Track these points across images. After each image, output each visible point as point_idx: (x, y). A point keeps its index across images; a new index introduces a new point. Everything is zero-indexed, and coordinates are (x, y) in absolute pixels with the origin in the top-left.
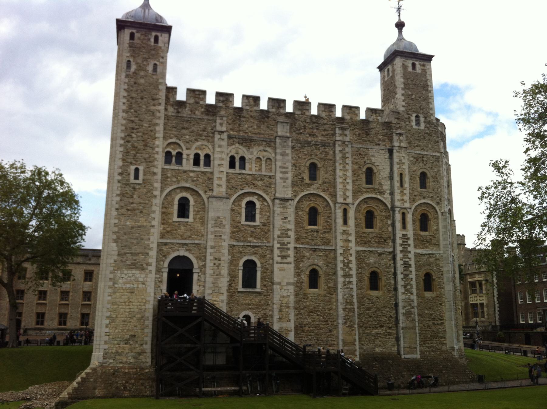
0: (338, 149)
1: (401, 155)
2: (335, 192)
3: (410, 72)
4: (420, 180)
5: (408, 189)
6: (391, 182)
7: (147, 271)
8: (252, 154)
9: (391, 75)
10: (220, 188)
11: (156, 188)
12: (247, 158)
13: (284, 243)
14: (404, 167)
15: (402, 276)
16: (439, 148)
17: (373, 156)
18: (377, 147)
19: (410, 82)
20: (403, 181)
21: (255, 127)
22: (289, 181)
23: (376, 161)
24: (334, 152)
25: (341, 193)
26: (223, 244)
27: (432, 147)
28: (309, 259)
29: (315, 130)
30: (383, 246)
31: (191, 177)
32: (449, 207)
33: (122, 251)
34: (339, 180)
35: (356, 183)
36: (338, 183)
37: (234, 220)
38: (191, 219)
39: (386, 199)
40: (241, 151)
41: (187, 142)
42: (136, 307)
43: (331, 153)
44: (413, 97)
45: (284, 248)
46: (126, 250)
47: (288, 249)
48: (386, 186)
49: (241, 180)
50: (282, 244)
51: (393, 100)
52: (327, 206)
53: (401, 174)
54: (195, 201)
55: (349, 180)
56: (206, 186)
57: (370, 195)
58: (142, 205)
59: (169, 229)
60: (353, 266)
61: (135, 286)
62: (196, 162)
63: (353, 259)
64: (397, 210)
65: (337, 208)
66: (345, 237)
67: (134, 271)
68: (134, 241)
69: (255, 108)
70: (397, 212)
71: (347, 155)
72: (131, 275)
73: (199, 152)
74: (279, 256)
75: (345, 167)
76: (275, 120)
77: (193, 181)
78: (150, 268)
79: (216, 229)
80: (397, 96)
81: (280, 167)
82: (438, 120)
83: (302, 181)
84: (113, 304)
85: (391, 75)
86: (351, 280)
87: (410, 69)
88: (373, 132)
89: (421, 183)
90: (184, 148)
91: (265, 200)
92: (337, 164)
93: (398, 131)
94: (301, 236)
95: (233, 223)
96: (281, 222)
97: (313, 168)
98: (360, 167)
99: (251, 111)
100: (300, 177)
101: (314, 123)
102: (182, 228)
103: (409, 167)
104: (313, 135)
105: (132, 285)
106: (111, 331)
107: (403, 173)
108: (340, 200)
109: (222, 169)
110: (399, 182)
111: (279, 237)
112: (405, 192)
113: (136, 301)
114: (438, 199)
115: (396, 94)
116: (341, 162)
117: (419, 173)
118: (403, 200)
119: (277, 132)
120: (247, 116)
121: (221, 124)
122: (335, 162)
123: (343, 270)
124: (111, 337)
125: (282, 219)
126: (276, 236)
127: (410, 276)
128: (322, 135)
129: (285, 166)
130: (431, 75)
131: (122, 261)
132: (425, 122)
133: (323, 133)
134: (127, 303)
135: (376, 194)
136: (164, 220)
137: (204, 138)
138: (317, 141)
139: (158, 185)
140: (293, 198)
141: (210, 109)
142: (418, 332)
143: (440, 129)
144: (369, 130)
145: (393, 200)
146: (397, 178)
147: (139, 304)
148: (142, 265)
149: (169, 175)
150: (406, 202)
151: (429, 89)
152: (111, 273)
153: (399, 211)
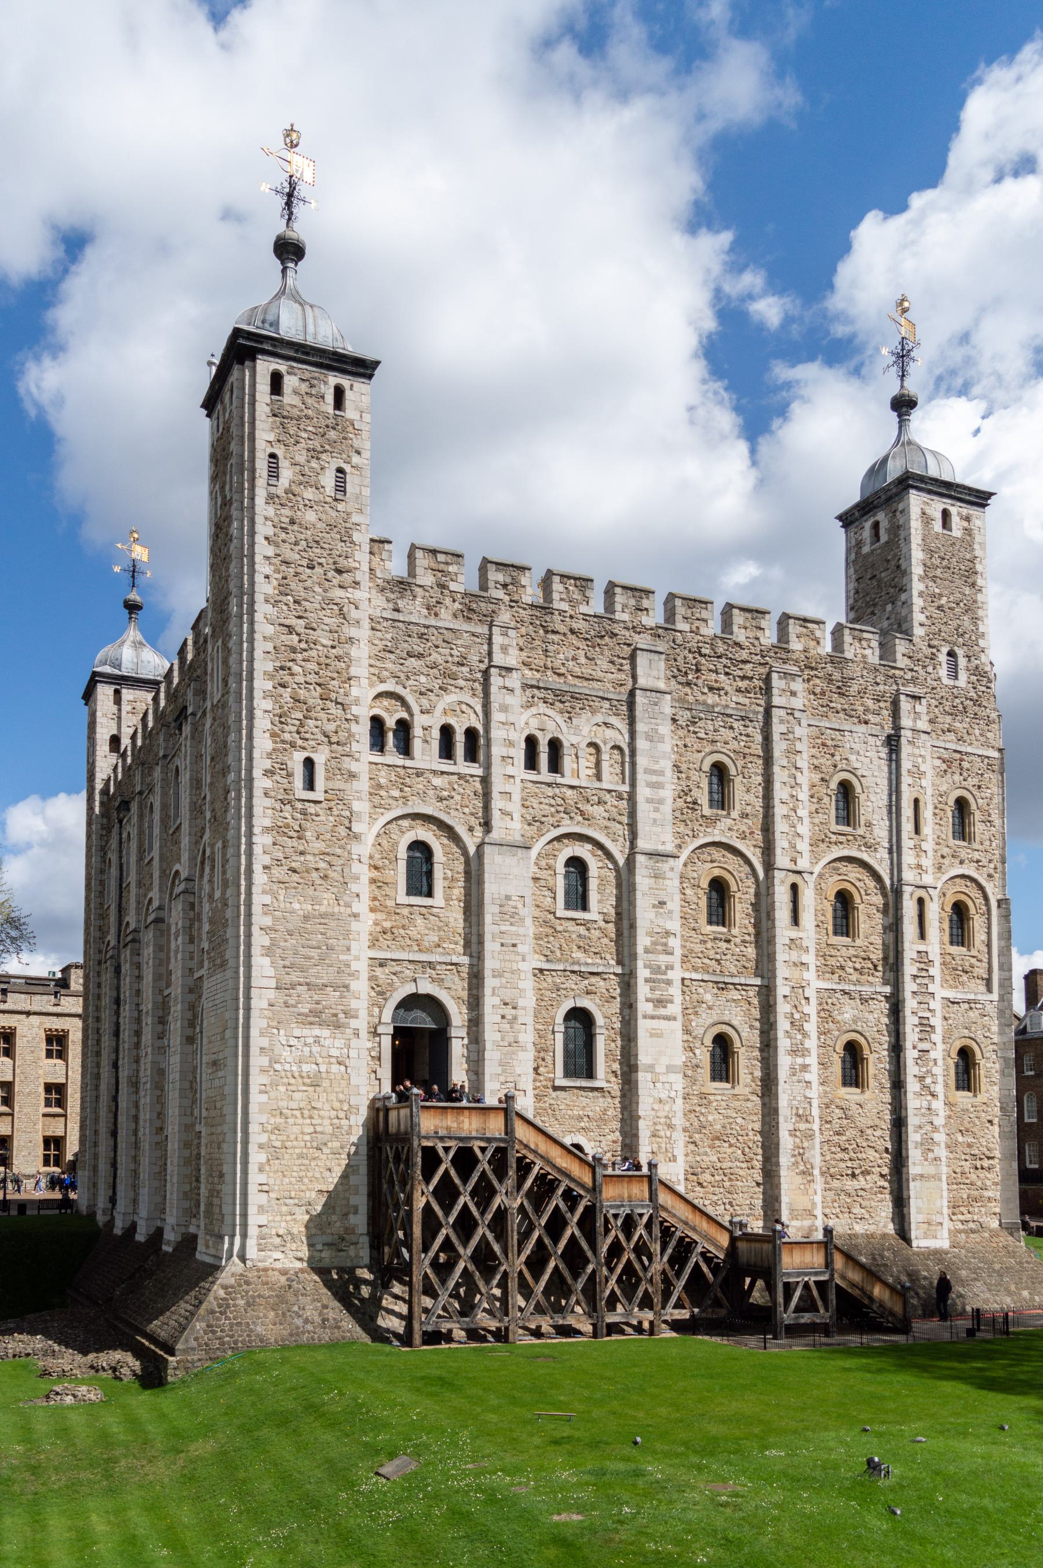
0: (777, 728)
1: (917, 751)
5: (930, 839)
7: (349, 1031)
8: (577, 730)
10: (508, 818)
11: (359, 814)
12: (566, 744)
13: (659, 967)
15: (916, 1054)
18: (862, 728)
21: (583, 660)
22: (667, 808)
25: (786, 845)
26: (522, 966)
28: (710, 1008)
30: (870, 979)
31: (435, 788)
33: (287, 979)
35: (816, 821)
37: (538, 906)
38: (438, 899)
40: (549, 722)
41: (421, 694)
42: (327, 1122)
43: (759, 738)
45: (659, 981)
46: (295, 977)
47: (669, 982)
49: (553, 802)
50: (656, 970)
51: (889, 607)
53: (916, 801)
54: (446, 854)
56: (472, 814)
58: (327, 858)
59: (387, 925)
60: (811, 1027)
61: (323, 1068)
62: (447, 751)
63: (811, 1009)
64: (907, 890)
66: (794, 956)
67: (317, 1031)
68: (314, 953)
69: (583, 609)
70: (906, 896)
71: (799, 746)
72: (310, 1040)
73: (452, 721)
74: (647, 1000)
76: (629, 645)
77: (441, 799)
78: (354, 1023)
79: (503, 928)
80: (903, 597)
81: (647, 771)
84: (272, 1112)
86: (808, 1061)
88: (854, 689)
90: (416, 709)
91: (609, 855)
92: (776, 769)
94: (691, 951)
95: (537, 913)
96: (651, 914)
97: (719, 771)
98: (823, 780)
99: (571, 617)
100: (689, 799)
101: (719, 657)
102: (420, 921)
105: (314, 1066)
106: (271, 1182)
107: (921, 799)
109: (510, 770)
111: (647, 951)
112: (925, 846)
113: (327, 1107)
117: (951, 802)
118: (919, 866)
119: (634, 677)
120: (562, 628)
121: (504, 649)
123: (791, 1038)
124: (273, 1195)
125: (654, 906)
126: (640, 950)
127: (933, 1055)
128: (739, 690)
129: (656, 767)
131: (287, 1005)
133: (740, 684)
134: (306, 1113)
136: (375, 899)
137: (461, 683)
139: (362, 806)
140: (675, 851)
141: (474, 606)
142: (945, 1186)
144: (846, 681)
145: (896, 866)
146: (907, 811)
147: (333, 1114)
148: (335, 1015)
149: (383, 781)
152: (262, 1034)
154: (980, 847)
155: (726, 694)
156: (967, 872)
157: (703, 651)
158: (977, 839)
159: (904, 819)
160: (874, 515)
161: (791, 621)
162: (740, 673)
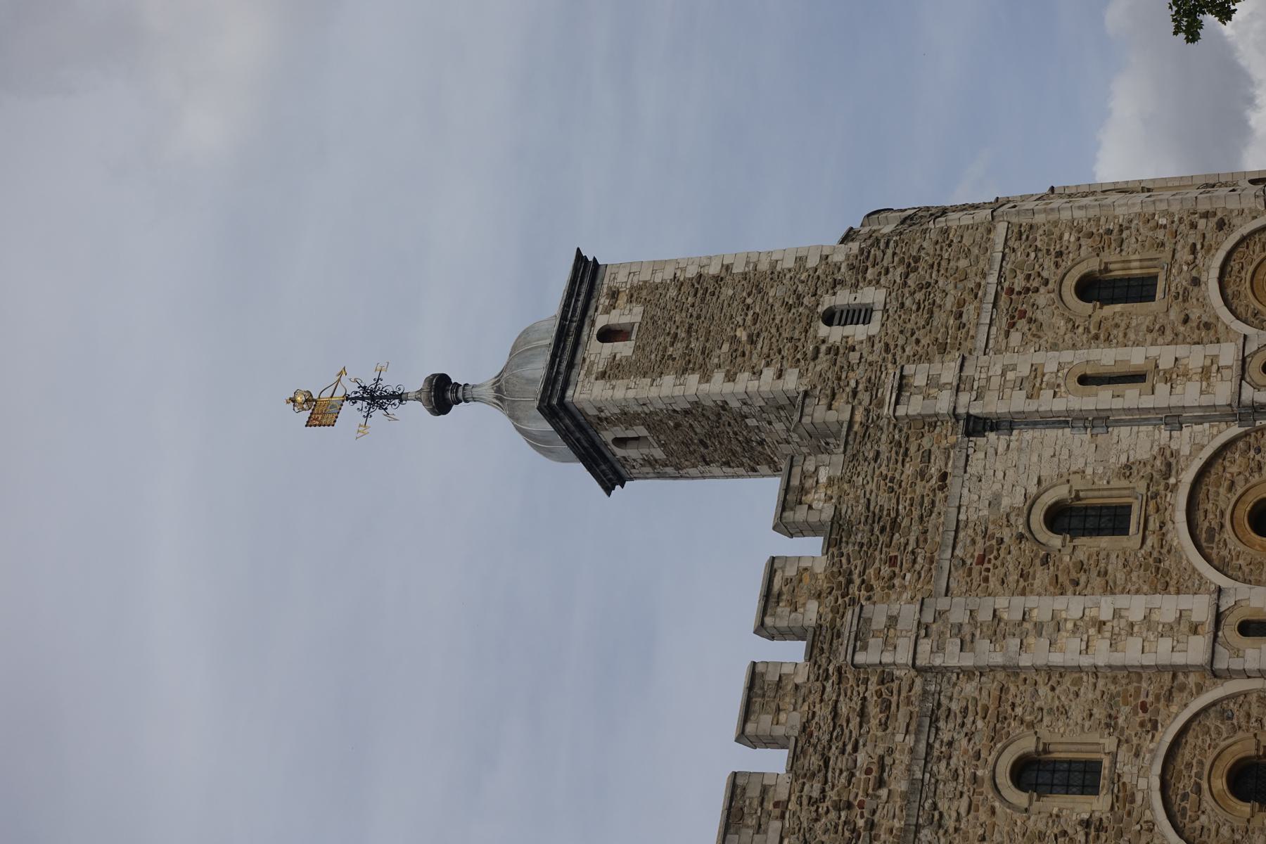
0: (952, 657)
1: (996, 382)
2: (1160, 669)
3: (637, 348)
4: (1114, 301)
5: (1154, 351)
6: (1119, 423)
9: (641, 431)
14: (1051, 367)
16: (975, 227)
17: (994, 503)
18: (954, 484)
19: (677, 350)
20: (1121, 370)
23: (1020, 491)
24: (968, 673)
25: (1165, 644)
27: (968, 253)
29: (861, 757)
32: (1244, 184)
34: (1102, 654)
35: (1121, 576)
36: (1117, 659)
39: (1194, 444)
43: (970, 688)
44: (742, 334)
48: (1138, 443)
51: (751, 422)
52: (1226, 716)
53: (1084, 380)
55: (1105, 607)
57: (1181, 517)
64: (1248, 394)
65: (1236, 664)
71: (985, 616)
75: (1039, 628)
82: (849, 236)
83: (1100, 828)
85: (641, 431)
87: (624, 349)
89: (1126, 300)
92: (1025, 660)
93: (888, 395)
97: (1034, 773)
98: (1045, 561)
101: (826, 762)
103: (1054, 347)
104: (882, 768)
107: (1079, 372)
108: (1196, 651)
110: (1120, 387)
112: (1166, 363)
114: (1202, 223)
115: (724, 406)
116: (1014, 643)
118: (1205, 373)
122: (1013, 671)
128: (884, 725)
130: (657, 266)
132: (856, 286)
133: (874, 722)
135: (1173, 489)
138: (912, 751)
143: (887, 229)
144: (873, 517)
145: (1208, 415)
150: (1214, 359)
151: (714, 270)
153: (1257, 387)
154: (1168, 248)
155: (890, 751)
156: (1215, 273)
157: (816, 794)
158: (1152, 254)
159: (1118, 404)
160: (606, 445)
161: (769, 621)
162: (855, 721)
